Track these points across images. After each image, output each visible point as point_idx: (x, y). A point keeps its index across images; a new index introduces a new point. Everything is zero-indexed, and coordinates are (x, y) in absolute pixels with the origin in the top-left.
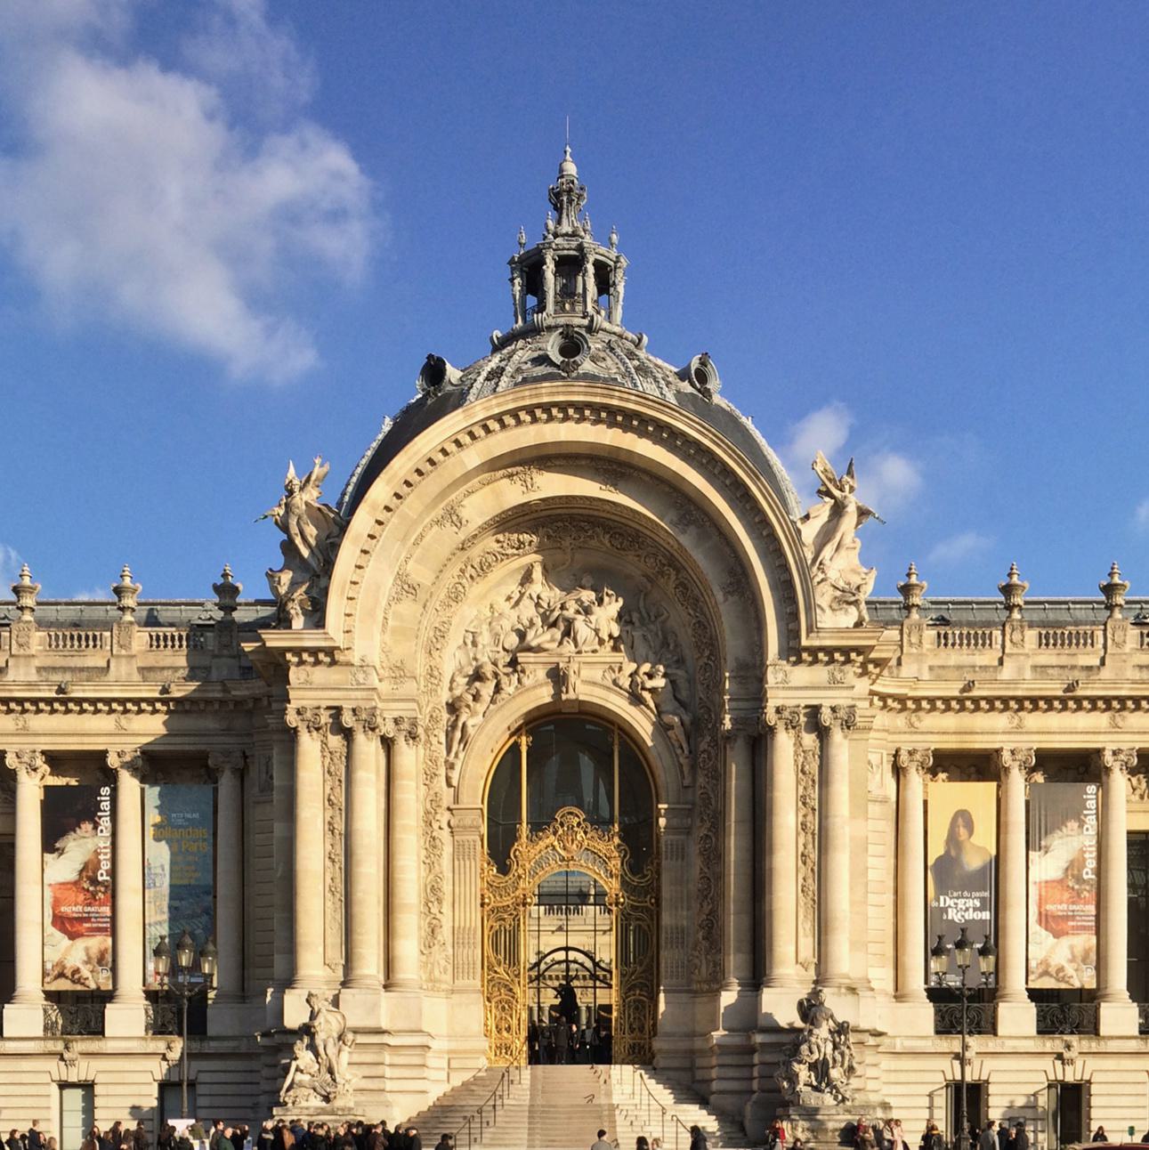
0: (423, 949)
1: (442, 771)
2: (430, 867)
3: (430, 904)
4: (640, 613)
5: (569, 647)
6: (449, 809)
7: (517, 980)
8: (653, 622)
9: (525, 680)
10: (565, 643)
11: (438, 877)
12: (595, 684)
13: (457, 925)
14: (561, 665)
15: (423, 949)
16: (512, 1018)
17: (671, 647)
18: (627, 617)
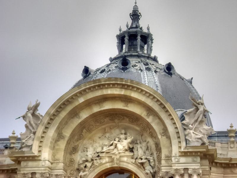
5: (115, 151)
9: (101, 162)
14: (113, 157)
17: (150, 150)
18: (135, 142)
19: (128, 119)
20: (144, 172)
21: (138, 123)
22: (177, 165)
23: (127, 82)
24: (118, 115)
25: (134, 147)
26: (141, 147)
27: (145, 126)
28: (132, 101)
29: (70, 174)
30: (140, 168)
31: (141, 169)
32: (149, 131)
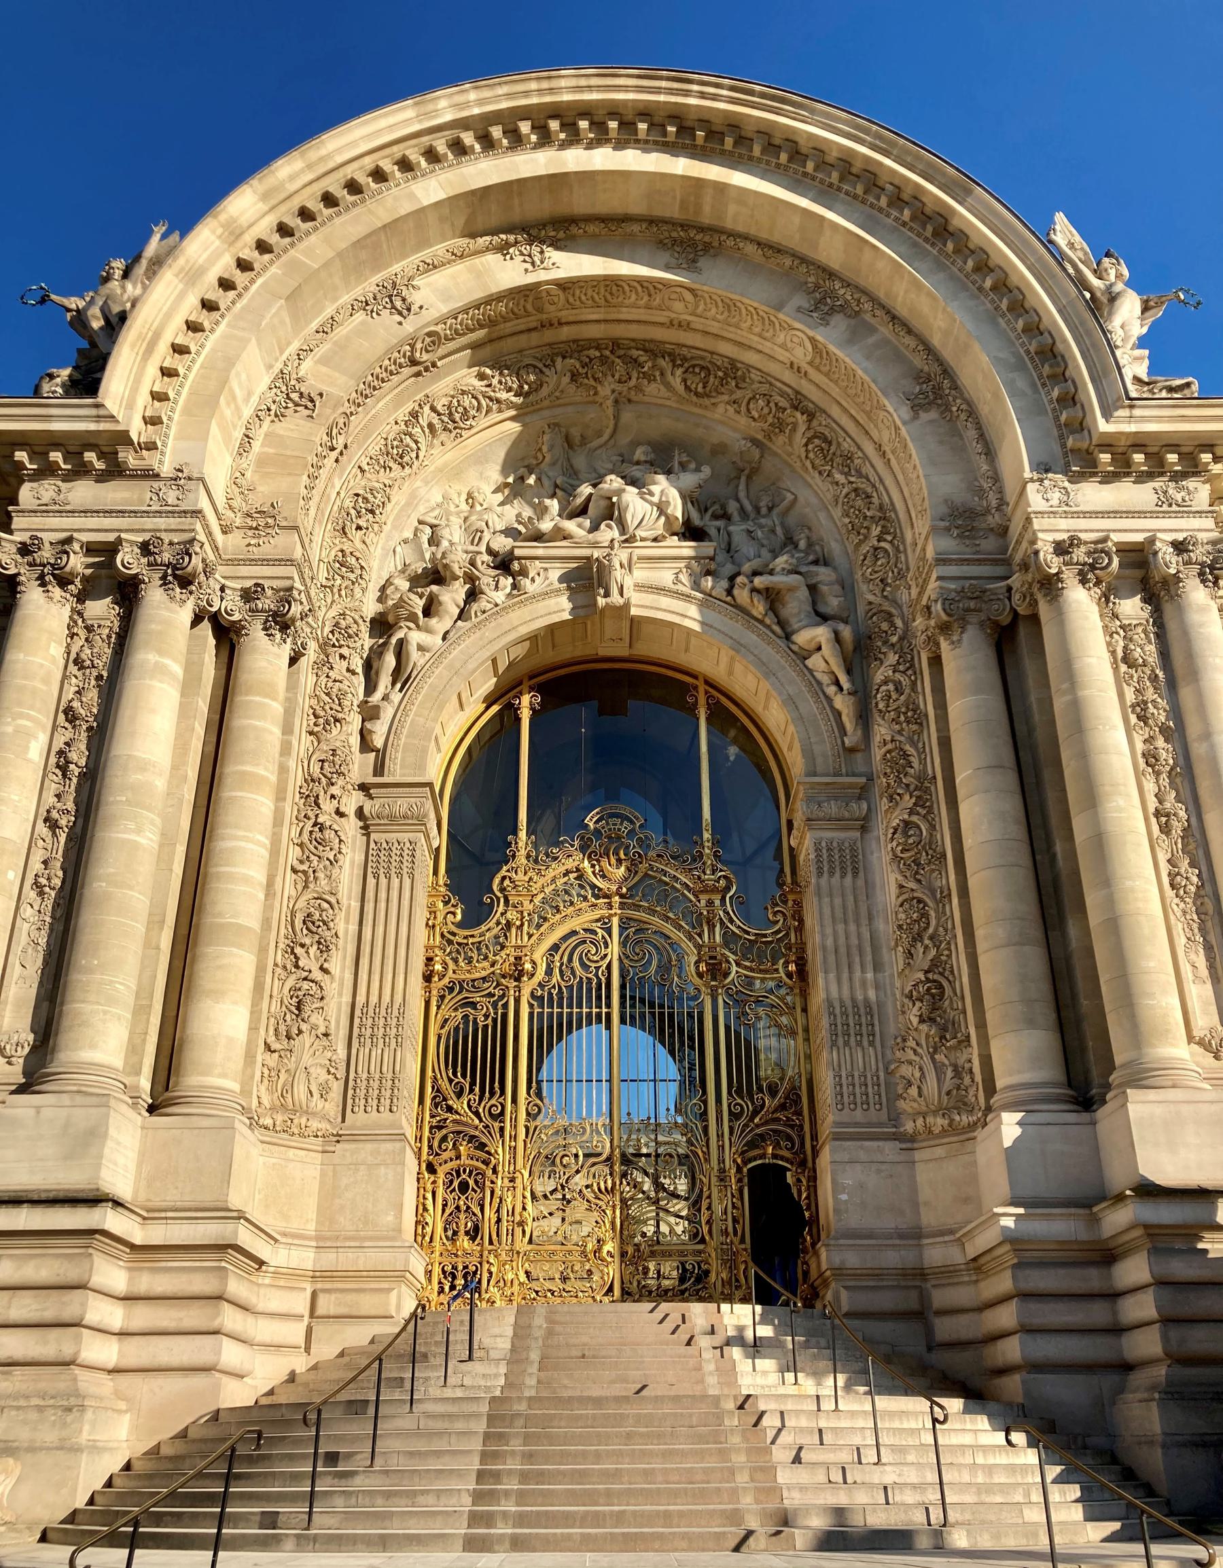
0: (271, 1039)
1: (355, 721)
2: (305, 877)
3: (298, 950)
4: (738, 500)
5: (608, 533)
6: (364, 788)
7: (497, 1125)
8: (764, 517)
10: (603, 526)
11: (328, 901)
12: (660, 590)
13: (361, 999)
15: (271, 1039)
16: (482, 1210)
17: (802, 544)
19: (679, 372)
20: (782, 643)
21: (739, 394)
22: (1063, 524)
23: (715, 97)
24: (622, 352)
25: (713, 532)
26: (749, 532)
27: (783, 403)
28: (723, 237)
29: (332, 632)
30: (761, 622)
31: (768, 627)
32: (809, 428)
